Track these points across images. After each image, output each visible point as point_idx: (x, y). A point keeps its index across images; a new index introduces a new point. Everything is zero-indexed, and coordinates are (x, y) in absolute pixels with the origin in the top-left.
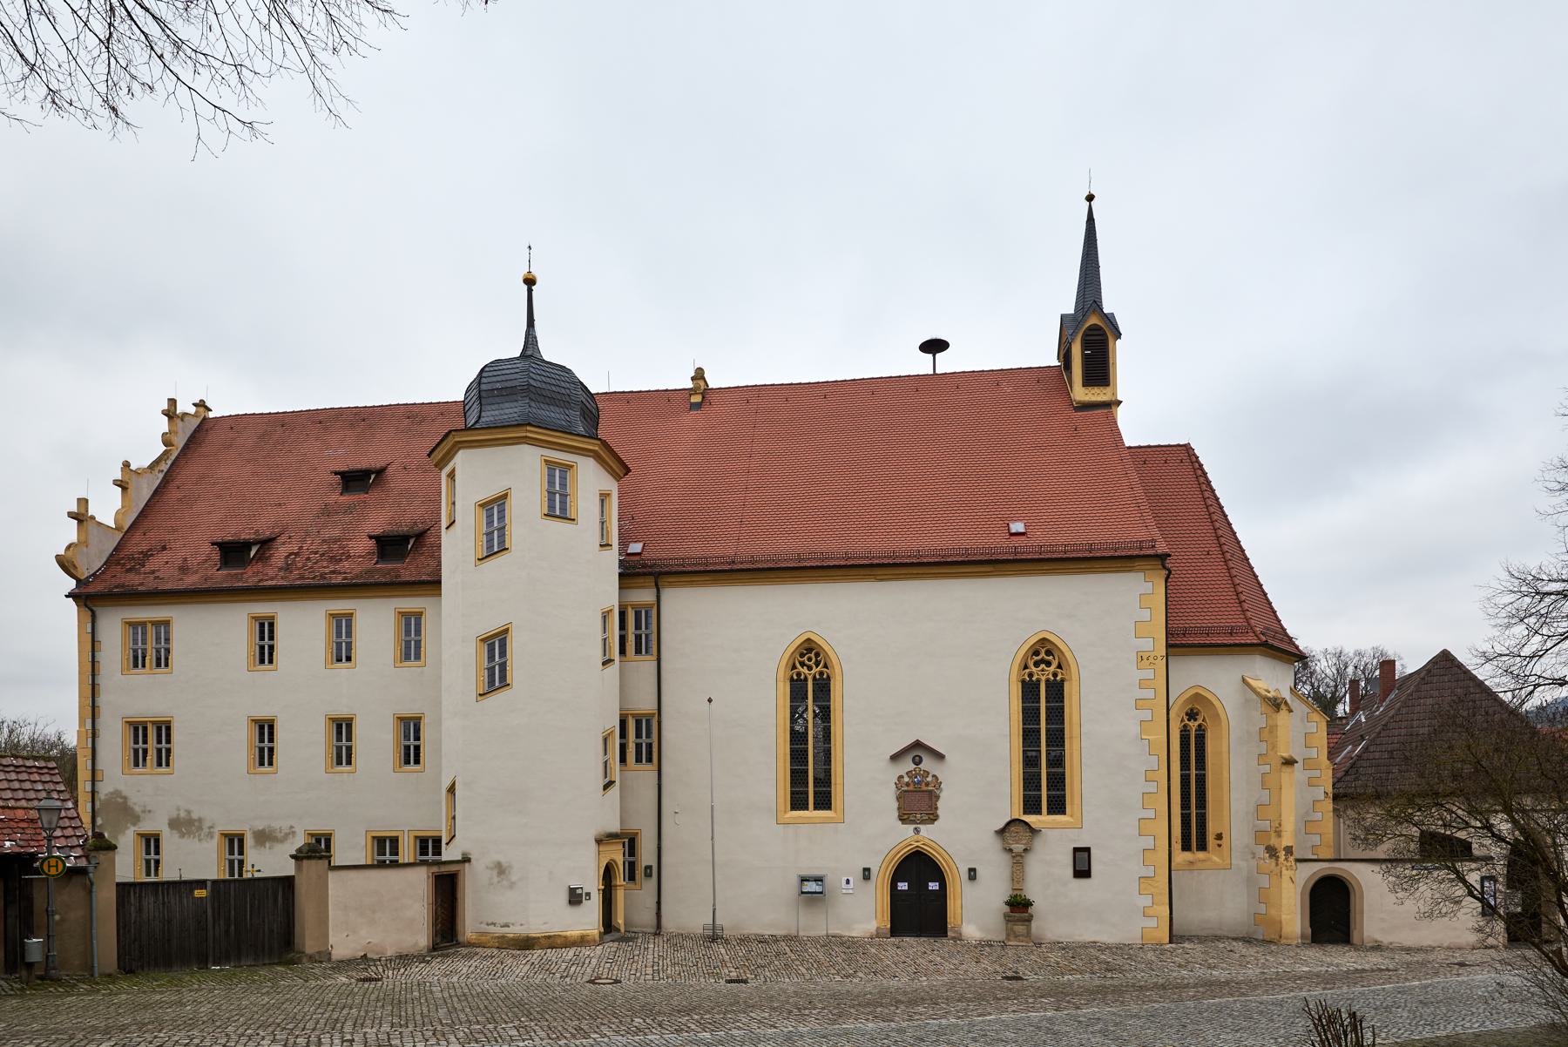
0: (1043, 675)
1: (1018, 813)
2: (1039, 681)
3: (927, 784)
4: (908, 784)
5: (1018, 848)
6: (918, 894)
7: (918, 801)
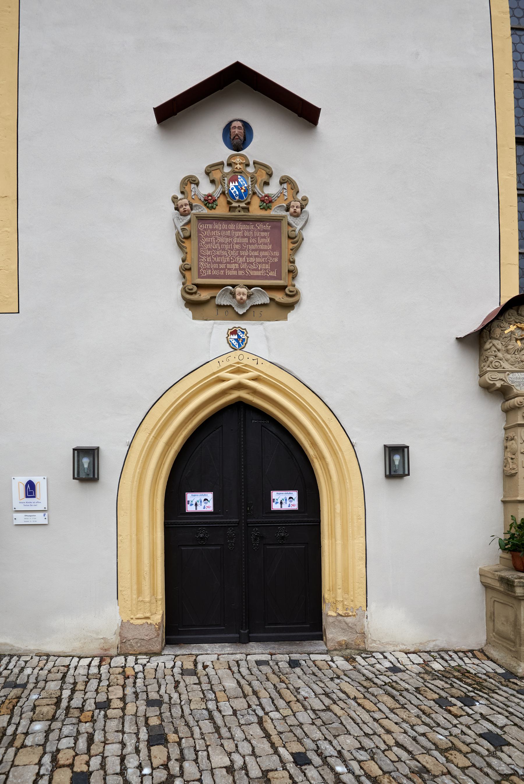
3: (267, 202)
4: (209, 201)
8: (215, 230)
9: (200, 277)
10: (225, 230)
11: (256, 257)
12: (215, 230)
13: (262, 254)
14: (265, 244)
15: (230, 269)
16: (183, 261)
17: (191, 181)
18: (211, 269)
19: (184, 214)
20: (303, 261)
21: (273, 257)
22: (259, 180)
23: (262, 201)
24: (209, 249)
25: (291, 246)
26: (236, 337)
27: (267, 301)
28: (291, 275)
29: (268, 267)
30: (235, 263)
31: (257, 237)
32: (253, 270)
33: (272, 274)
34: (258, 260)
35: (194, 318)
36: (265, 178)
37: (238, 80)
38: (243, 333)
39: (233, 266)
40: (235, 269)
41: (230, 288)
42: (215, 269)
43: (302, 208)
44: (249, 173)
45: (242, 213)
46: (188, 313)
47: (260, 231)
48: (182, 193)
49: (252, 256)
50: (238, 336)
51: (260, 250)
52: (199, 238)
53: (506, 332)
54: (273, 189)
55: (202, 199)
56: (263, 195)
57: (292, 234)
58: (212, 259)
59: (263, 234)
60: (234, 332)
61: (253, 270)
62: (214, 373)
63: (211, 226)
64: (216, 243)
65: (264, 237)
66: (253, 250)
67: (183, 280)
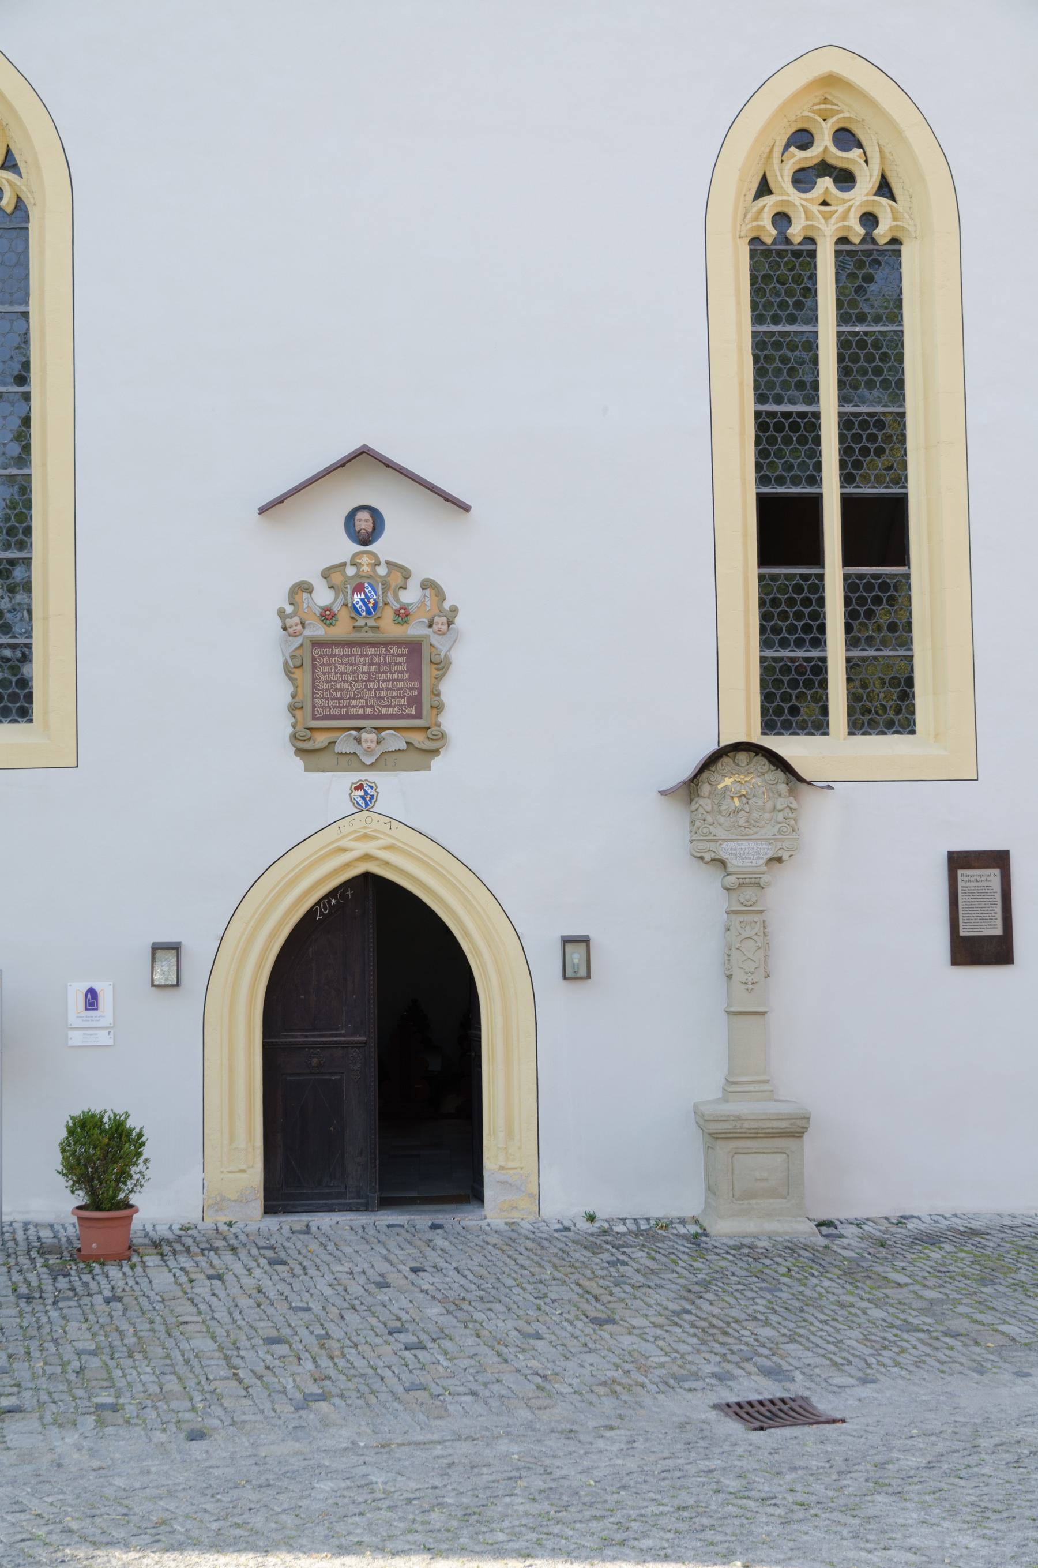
0: (826, 221)
1: (744, 723)
2: (806, 254)
3: (403, 615)
4: (327, 616)
5: (746, 854)
6: (379, 1044)
7: (367, 677)
8: (335, 656)
9: (314, 718)
10: (348, 656)
11: (388, 689)
12: (335, 656)
13: (397, 685)
14: (401, 672)
15: (354, 707)
16: (293, 697)
17: (303, 588)
18: (329, 707)
19: (295, 635)
20: (451, 690)
21: (411, 689)
22: (393, 584)
23: (397, 613)
24: (327, 682)
25: (436, 673)
26: (362, 793)
27: (403, 746)
28: (435, 711)
29: (403, 702)
30: (361, 698)
31: (390, 664)
32: (384, 706)
33: (411, 711)
34: (391, 693)
35: (307, 770)
36: (400, 581)
37: (364, 458)
38: (372, 787)
39: (358, 703)
40: (361, 707)
41: (354, 733)
42: (334, 707)
43: (450, 623)
44: (380, 577)
45: (370, 634)
46: (299, 763)
47: (393, 655)
48: (291, 604)
49: (383, 689)
50: (366, 793)
51: (394, 681)
52: (314, 667)
53: (720, 787)
54: (411, 596)
55: (318, 614)
56: (398, 606)
57: (435, 659)
58: (331, 694)
59: (397, 659)
60: (360, 787)
61: (384, 706)
62: (333, 842)
63: (329, 651)
64: (336, 673)
65: (400, 664)
66: (384, 681)
67: (293, 720)
